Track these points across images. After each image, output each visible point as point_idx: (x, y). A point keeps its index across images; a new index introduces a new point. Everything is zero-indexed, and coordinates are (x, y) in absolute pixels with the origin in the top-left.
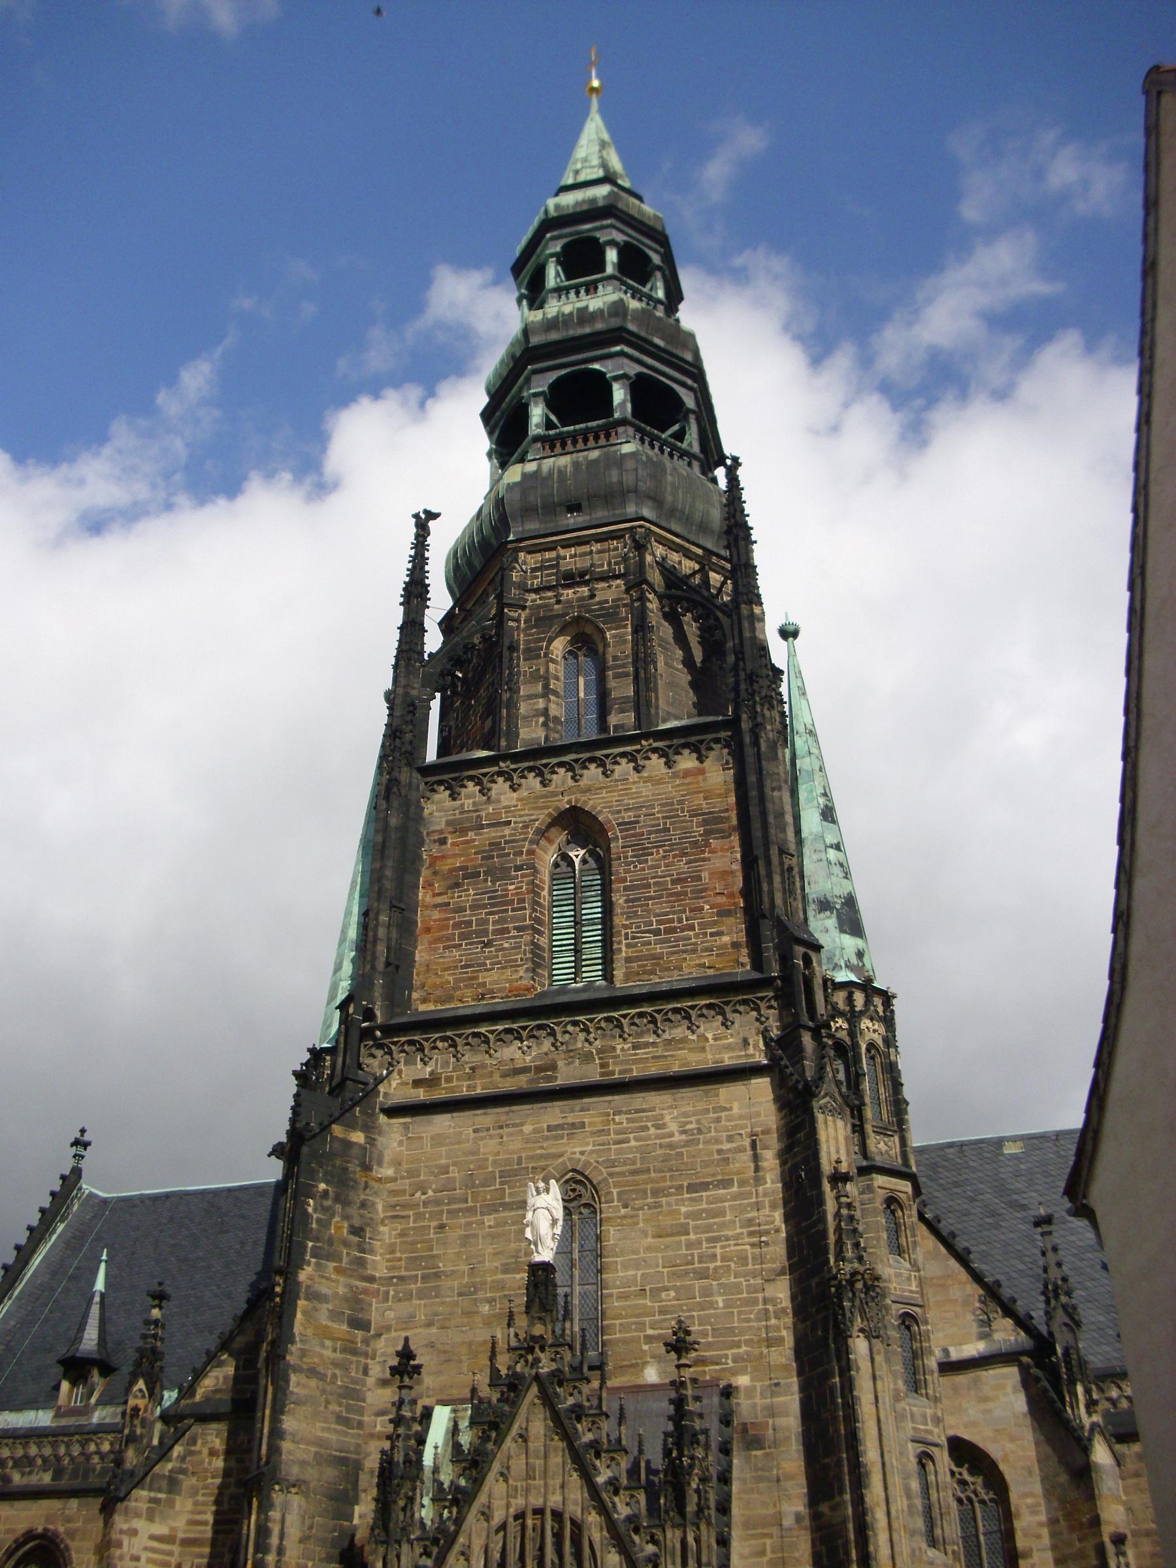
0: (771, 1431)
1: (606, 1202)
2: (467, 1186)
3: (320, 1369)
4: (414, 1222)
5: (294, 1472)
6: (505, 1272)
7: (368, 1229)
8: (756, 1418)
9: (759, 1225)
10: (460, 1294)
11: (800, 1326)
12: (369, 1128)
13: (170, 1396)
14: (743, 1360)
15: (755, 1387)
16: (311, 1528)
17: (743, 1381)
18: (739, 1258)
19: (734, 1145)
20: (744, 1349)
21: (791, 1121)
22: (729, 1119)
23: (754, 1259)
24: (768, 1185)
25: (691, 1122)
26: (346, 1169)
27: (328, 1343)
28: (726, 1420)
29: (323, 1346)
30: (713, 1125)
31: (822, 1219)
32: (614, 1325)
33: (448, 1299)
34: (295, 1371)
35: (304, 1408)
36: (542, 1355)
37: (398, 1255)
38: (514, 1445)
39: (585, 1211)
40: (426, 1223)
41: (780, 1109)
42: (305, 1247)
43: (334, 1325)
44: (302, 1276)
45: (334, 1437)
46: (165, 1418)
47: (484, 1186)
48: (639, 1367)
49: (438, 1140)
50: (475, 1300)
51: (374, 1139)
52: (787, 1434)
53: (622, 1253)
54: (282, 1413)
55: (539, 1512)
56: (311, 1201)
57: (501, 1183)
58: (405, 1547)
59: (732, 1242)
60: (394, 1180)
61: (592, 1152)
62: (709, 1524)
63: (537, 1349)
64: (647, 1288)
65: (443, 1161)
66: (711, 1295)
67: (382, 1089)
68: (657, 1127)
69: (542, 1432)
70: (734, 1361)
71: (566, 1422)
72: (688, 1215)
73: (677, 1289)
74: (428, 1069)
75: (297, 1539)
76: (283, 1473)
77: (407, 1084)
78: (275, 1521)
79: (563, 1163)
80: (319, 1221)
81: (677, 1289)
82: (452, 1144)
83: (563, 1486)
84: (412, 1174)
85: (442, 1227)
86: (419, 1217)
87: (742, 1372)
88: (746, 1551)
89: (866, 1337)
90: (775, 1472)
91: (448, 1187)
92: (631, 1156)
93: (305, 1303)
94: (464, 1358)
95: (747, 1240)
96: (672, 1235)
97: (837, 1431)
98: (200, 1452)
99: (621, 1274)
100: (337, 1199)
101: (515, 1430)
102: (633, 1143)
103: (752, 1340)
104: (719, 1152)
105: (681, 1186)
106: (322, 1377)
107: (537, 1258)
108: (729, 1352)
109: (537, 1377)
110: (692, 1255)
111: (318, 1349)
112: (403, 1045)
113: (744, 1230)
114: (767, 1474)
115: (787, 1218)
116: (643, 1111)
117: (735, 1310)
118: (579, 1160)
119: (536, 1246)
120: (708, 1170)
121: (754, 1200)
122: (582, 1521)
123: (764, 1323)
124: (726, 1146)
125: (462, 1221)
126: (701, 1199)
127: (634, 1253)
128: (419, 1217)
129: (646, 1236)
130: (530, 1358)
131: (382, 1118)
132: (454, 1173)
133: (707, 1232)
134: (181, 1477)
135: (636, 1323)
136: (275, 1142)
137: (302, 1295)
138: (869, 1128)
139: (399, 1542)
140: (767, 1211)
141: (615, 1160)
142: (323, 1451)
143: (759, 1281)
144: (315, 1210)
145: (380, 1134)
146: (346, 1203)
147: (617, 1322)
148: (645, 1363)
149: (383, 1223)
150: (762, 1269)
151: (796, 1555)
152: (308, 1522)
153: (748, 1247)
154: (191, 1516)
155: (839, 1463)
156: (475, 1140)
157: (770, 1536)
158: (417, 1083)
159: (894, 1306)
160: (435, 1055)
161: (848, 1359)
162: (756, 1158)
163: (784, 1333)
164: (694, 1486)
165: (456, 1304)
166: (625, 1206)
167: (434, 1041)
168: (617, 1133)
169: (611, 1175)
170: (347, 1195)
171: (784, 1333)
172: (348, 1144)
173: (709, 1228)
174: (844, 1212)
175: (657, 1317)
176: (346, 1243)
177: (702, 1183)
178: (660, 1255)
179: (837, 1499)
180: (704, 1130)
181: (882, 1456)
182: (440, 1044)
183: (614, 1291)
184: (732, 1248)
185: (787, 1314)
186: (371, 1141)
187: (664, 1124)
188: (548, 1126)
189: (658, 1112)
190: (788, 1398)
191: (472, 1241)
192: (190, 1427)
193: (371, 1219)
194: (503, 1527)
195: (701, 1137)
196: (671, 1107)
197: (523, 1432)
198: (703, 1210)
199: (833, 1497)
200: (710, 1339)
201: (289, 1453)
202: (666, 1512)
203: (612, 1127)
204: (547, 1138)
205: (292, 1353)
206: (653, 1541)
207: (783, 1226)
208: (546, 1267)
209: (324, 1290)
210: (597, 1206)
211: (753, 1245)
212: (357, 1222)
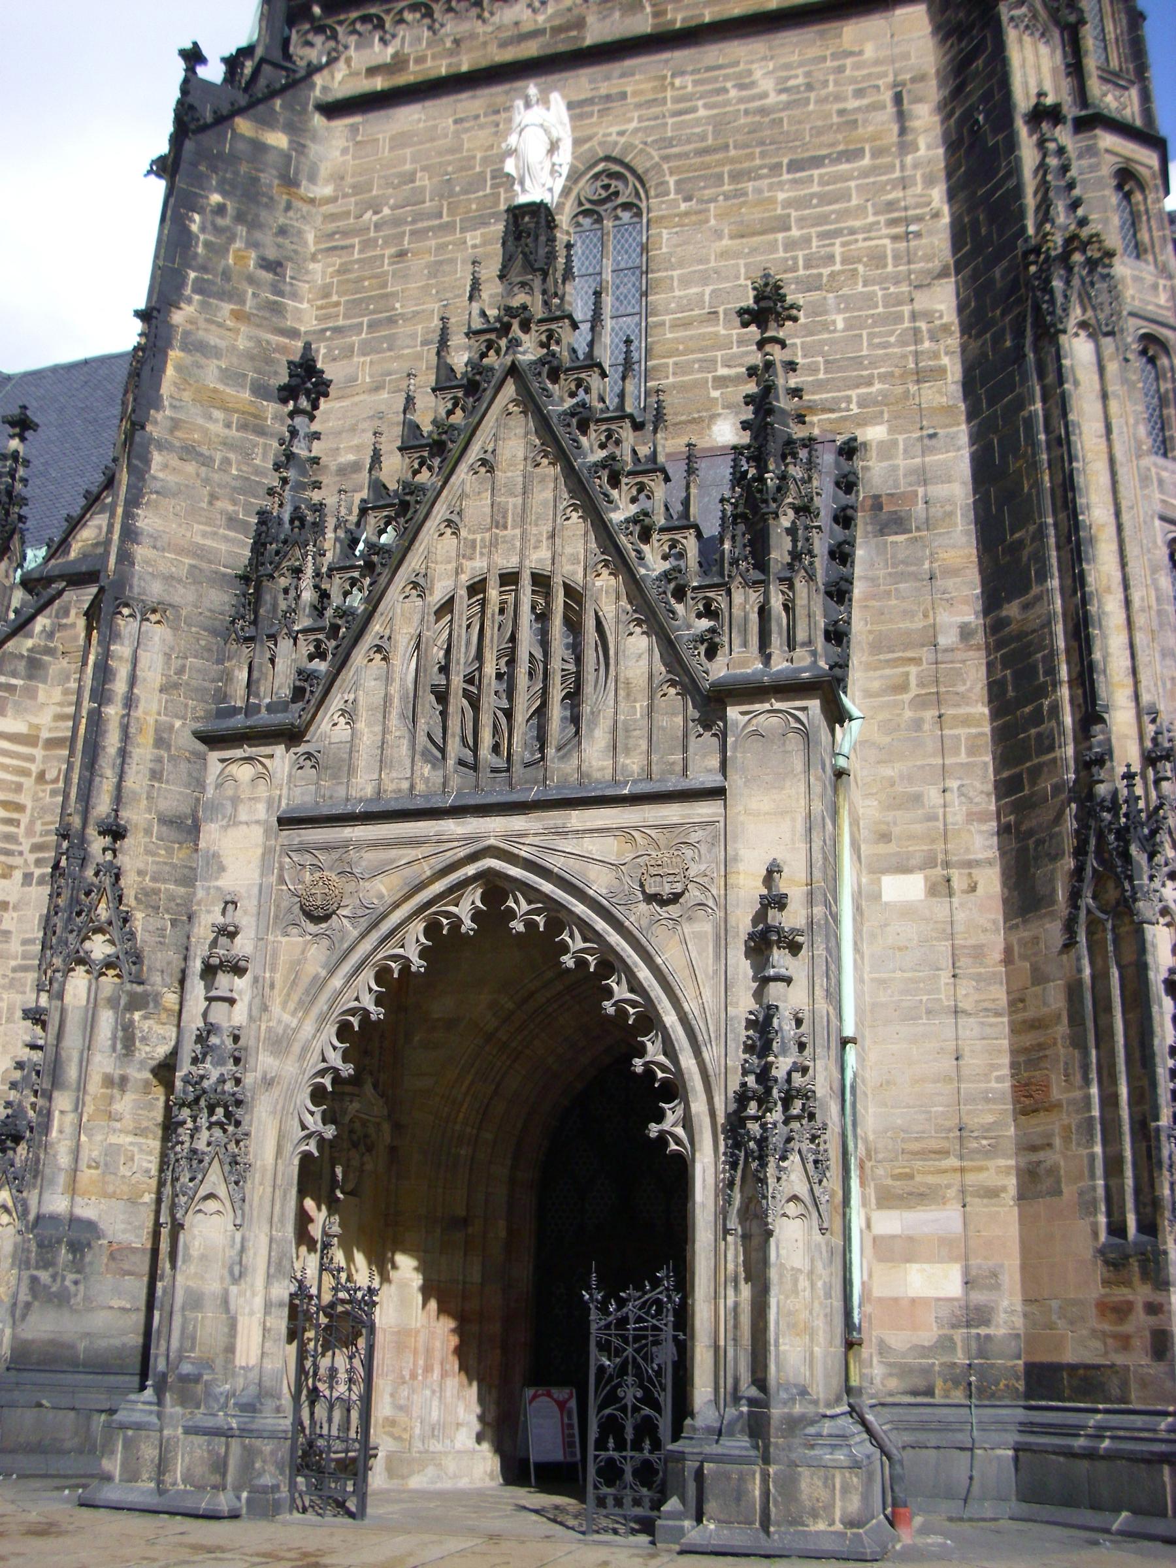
0: (921, 505)
1: (657, 196)
2: (441, 197)
3: (204, 449)
4: (361, 252)
5: (155, 590)
7: (289, 265)
8: (897, 487)
9: (906, 209)
11: (974, 345)
12: (294, 129)
13: (35, 557)
14: (876, 403)
15: (894, 443)
16: (180, 671)
17: (874, 434)
18: (871, 258)
19: (865, 102)
20: (877, 387)
21: (961, 51)
22: (857, 66)
23: (897, 257)
24: (922, 151)
25: (796, 76)
26: (257, 180)
27: (218, 414)
28: (847, 484)
29: (210, 418)
30: (831, 78)
31: (1015, 170)
32: (667, 365)
33: (406, 351)
34: (160, 447)
35: (173, 502)
36: (524, 337)
37: (335, 298)
38: (470, 477)
39: (626, 216)
40: (378, 252)
41: (944, 40)
42: (185, 277)
43: (228, 390)
44: (178, 317)
45: (223, 547)
46: (27, 583)
47: (465, 192)
48: (705, 421)
49: (399, 141)
51: (304, 146)
52: (948, 508)
53: (681, 264)
54: (137, 505)
55: (509, 579)
56: (197, 217)
57: (493, 186)
58: (285, 644)
59: (860, 237)
60: (333, 200)
61: (636, 130)
62: (811, 577)
63: (516, 327)
64: (721, 310)
65: (408, 167)
66: (826, 312)
67: (319, 80)
68: (741, 87)
69: (521, 454)
70: (860, 405)
71: (560, 431)
72: (788, 204)
74: (390, 50)
75: (157, 686)
76: (136, 590)
77: (358, 74)
78: (121, 658)
79: (591, 149)
80: (207, 244)
82: (421, 143)
83: (553, 536)
84: (357, 189)
85: (402, 254)
86: (367, 244)
87: (875, 419)
88: (876, 685)
89: (1090, 336)
90: (926, 566)
91: (416, 199)
93: (180, 354)
95: (885, 231)
97: (1037, 484)
98: (73, 625)
99: (677, 293)
100: (240, 218)
101: (474, 453)
103: (892, 374)
104: (841, 112)
105: (779, 165)
106: (207, 462)
107: (522, 199)
108: (854, 394)
109: (513, 370)
110: (795, 259)
111: (200, 421)
112: (353, 22)
113: (882, 219)
114: (913, 568)
115: (951, 196)
116: (720, 67)
117: (864, 333)
118: (616, 143)
119: (522, 183)
120: (825, 139)
121: (897, 174)
122: (585, 587)
123: (912, 348)
124: (852, 104)
126: (810, 179)
127: (701, 261)
128: (367, 244)
130: (503, 343)
131: (318, 120)
132: (424, 181)
134: (46, 658)
135: (700, 360)
136: (155, 156)
137: (176, 344)
138: (1091, 63)
139: (273, 637)
140: (919, 189)
141: (672, 138)
142: (204, 565)
143: (904, 288)
144: (203, 229)
145: (314, 139)
146: (254, 225)
147: (671, 361)
148: (713, 417)
149: (314, 258)
150: (910, 272)
151: (961, 689)
152: (176, 663)
153: (887, 241)
154: (58, 709)
155: (1040, 534)
156: (457, 134)
157: (916, 661)
158: (372, 71)
159: (1132, 322)
160: (401, 31)
161: (1060, 368)
162: (901, 116)
163: (945, 360)
164: (786, 522)
166: (688, 199)
167: (401, 12)
168: (677, 100)
169: (666, 158)
170: (257, 216)
171: (945, 360)
172: (259, 147)
173: (823, 219)
174: (1053, 162)
175: (735, 350)
176: (251, 280)
178: (742, 262)
179: (1035, 590)
181: (1118, 514)
182: (408, 16)
183: (667, 318)
184: (861, 244)
185: (951, 333)
186: (299, 147)
189: (742, 67)
190: (951, 454)
191: (446, 268)
192: (60, 593)
193: (295, 252)
194: (447, 607)
195: (813, 95)
196: (764, 59)
197: (488, 456)
198: (813, 195)
199: (1026, 589)
200: (821, 376)
201: (147, 562)
202: (735, 562)
205: (156, 423)
206: (709, 612)
207: (946, 209)
208: (538, 210)
209: (213, 340)
210: (643, 205)
211: (895, 238)
212: (271, 254)
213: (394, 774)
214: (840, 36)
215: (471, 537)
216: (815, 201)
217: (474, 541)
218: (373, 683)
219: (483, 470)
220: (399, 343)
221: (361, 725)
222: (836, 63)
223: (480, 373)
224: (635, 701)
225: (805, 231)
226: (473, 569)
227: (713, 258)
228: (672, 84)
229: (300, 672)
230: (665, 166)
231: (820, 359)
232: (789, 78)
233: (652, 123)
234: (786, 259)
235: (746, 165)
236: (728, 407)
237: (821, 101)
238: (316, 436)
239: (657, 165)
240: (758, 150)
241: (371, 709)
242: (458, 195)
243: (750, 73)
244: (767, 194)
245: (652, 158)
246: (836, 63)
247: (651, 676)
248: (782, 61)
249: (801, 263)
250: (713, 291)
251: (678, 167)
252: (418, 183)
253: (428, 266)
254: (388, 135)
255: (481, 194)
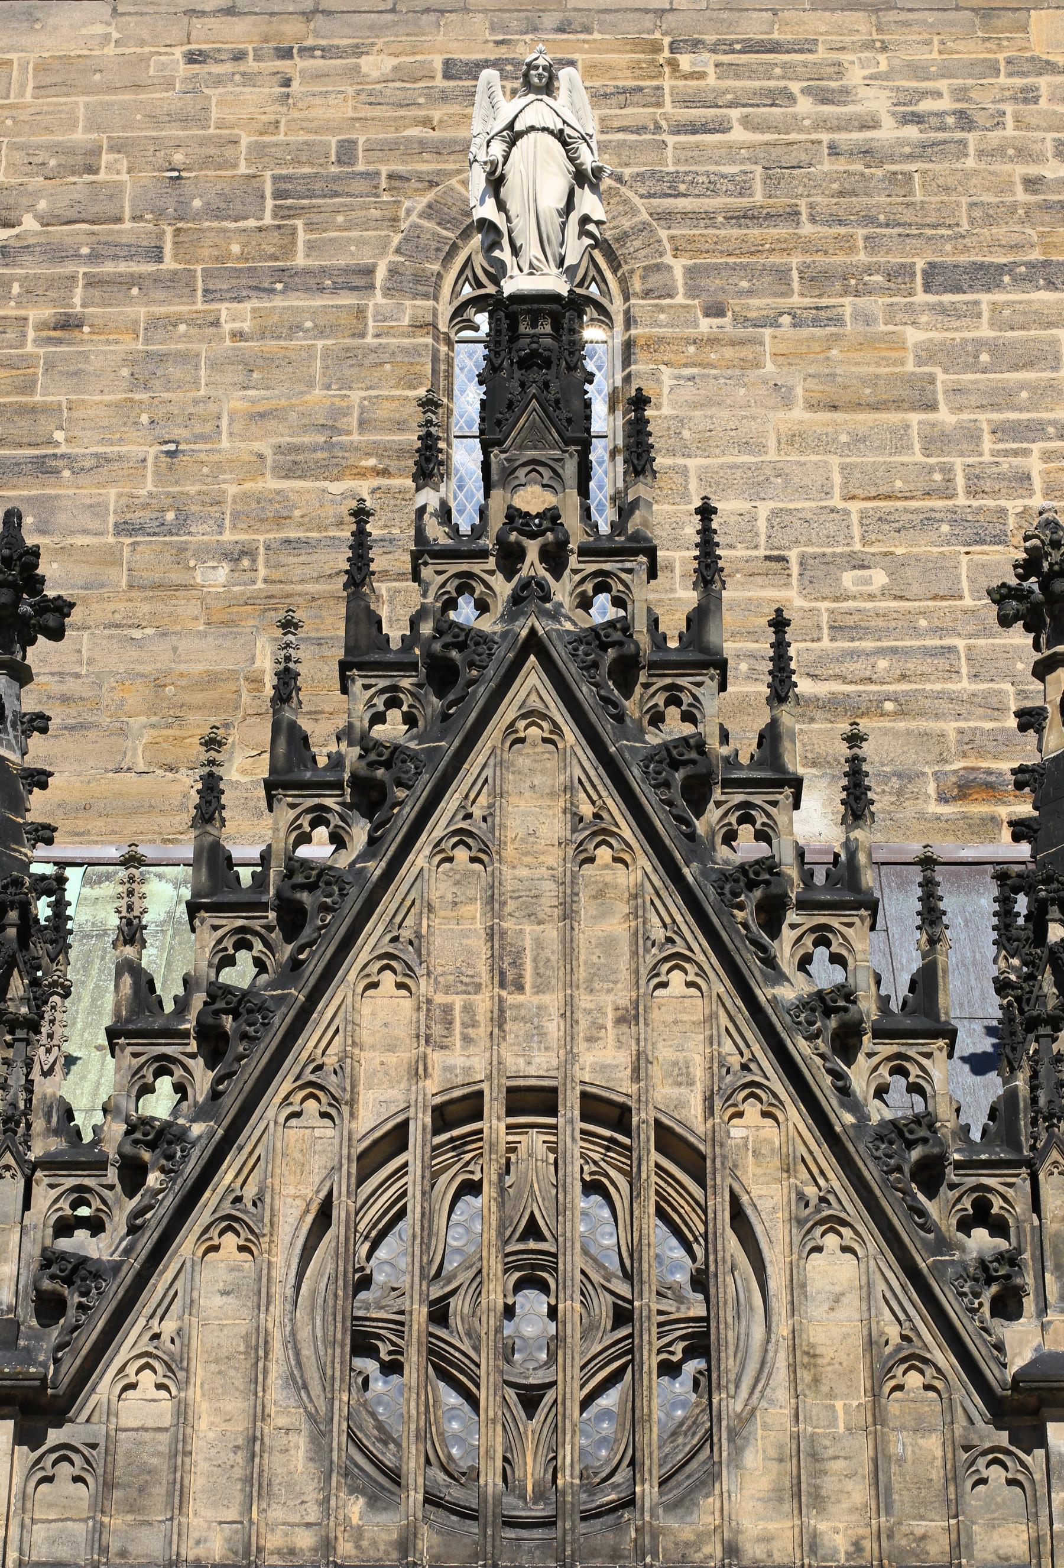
1: (647, 294)
2: (160, 214)
6: (290, 472)
10: (124, 528)
25: (939, 95)
30: (1009, 108)
33: (80, 540)
47: (217, 215)
50: (182, 549)
53: (703, 445)
64: (793, 555)
65: (80, 136)
68: (824, 97)
72: (928, 354)
73: (894, 565)
81: (894, 565)
85: (68, 324)
92: (734, 169)
94: (137, 722)
96: (876, 407)
102: (739, 134)
104: (1032, 184)
105: (907, 271)
110: (947, 470)
116: (774, 48)
120: (999, 231)
122: (713, 1138)
125: (142, 312)
126: (974, 312)
127: (746, 446)
129: (788, 403)
133: (994, 407)
141: (675, 178)
165: (111, 557)
166: (715, 310)
168: (688, 102)
169: (665, 217)
175: (826, 643)
177: (981, 266)
178: (835, 461)
180: (980, 118)
187: (845, 91)
188: (447, 63)
189: (822, 53)
191: (175, 372)
195: (971, 137)
196: (868, 46)
197: (476, 826)
198: (980, 344)
203: (667, 83)
204: (445, 97)
213: (277, 1513)
214: (1024, 28)
215: (439, 999)
216: (984, 357)
217: (448, 1009)
218: (219, 1301)
219: (462, 855)
220: (62, 518)
221: (194, 1394)
222: (1019, 82)
223: (461, 647)
224: (831, 1395)
225: (965, 416)
226: (448, 1069)
227: (772, 443)
228: (674, 65)
229: (49, 1259)
230: (663, 234)
231: (1007, 687)
232: (924, 94)
233: (634, 137)
234: (931, 470)
235: (839, 259)
236: (814, 764)
237: (996, 153)
238: (39, 723)
239: (645, 226)
240: (861, 232)
241: (220, 1360)
242: (196, 217)
243: (839, 71)
244: (883, 328)
245: (634, 211)
246: (1019, 82)
247: (871, 1343)
248: (905, 56)
249: (960, 481)
250: (775, 513)
251: (691, 241)
252: (102, 176)
253: (130, 360)
254: (33, 57)
255: (252, 223)
